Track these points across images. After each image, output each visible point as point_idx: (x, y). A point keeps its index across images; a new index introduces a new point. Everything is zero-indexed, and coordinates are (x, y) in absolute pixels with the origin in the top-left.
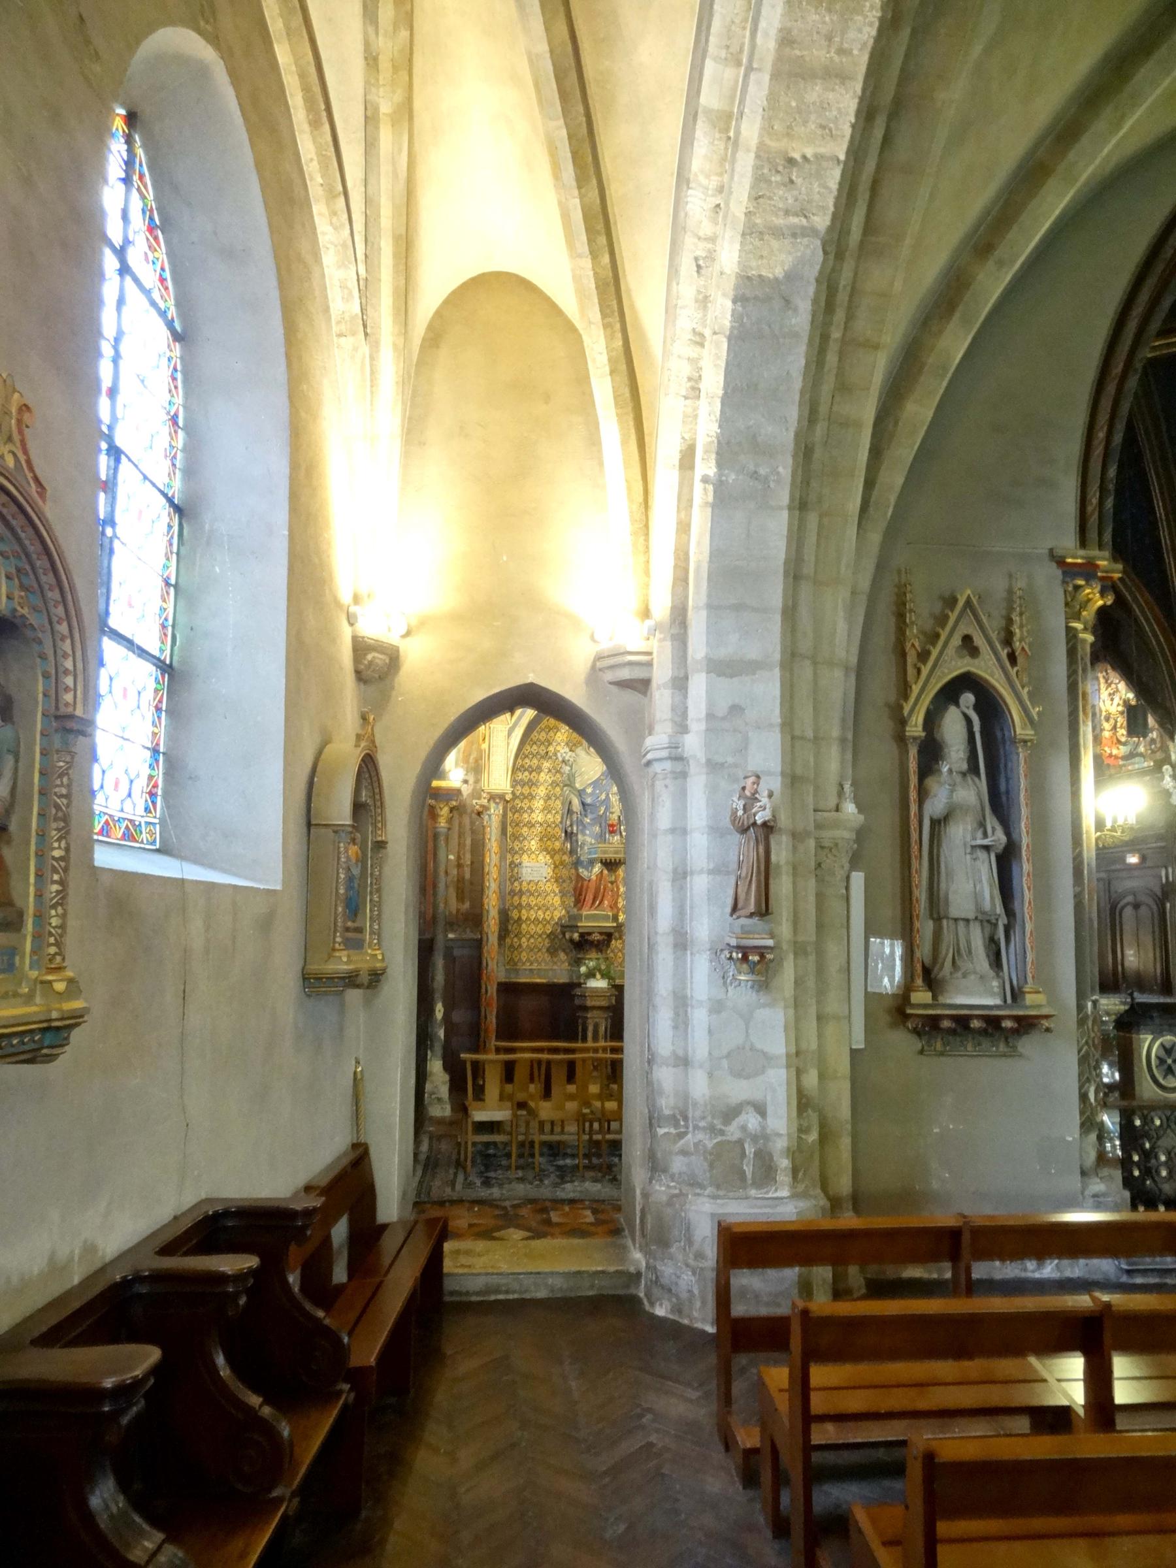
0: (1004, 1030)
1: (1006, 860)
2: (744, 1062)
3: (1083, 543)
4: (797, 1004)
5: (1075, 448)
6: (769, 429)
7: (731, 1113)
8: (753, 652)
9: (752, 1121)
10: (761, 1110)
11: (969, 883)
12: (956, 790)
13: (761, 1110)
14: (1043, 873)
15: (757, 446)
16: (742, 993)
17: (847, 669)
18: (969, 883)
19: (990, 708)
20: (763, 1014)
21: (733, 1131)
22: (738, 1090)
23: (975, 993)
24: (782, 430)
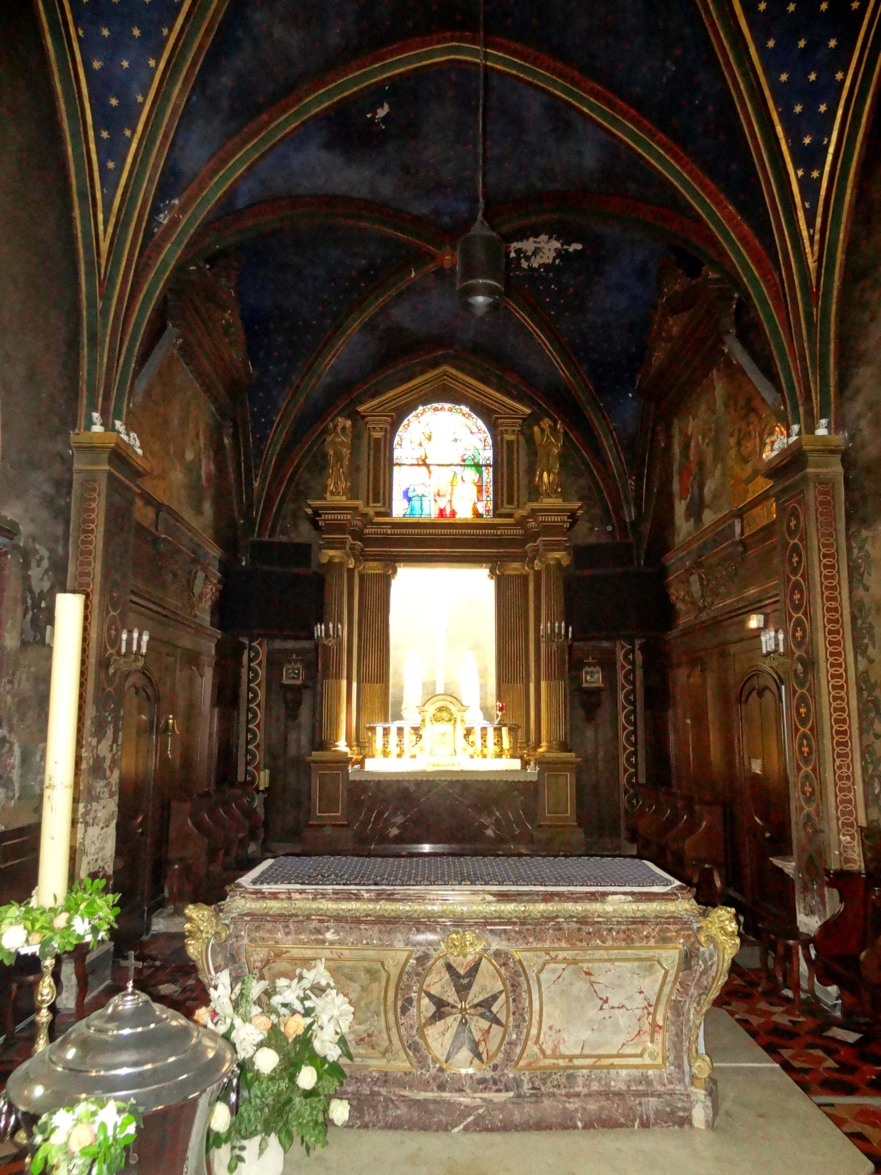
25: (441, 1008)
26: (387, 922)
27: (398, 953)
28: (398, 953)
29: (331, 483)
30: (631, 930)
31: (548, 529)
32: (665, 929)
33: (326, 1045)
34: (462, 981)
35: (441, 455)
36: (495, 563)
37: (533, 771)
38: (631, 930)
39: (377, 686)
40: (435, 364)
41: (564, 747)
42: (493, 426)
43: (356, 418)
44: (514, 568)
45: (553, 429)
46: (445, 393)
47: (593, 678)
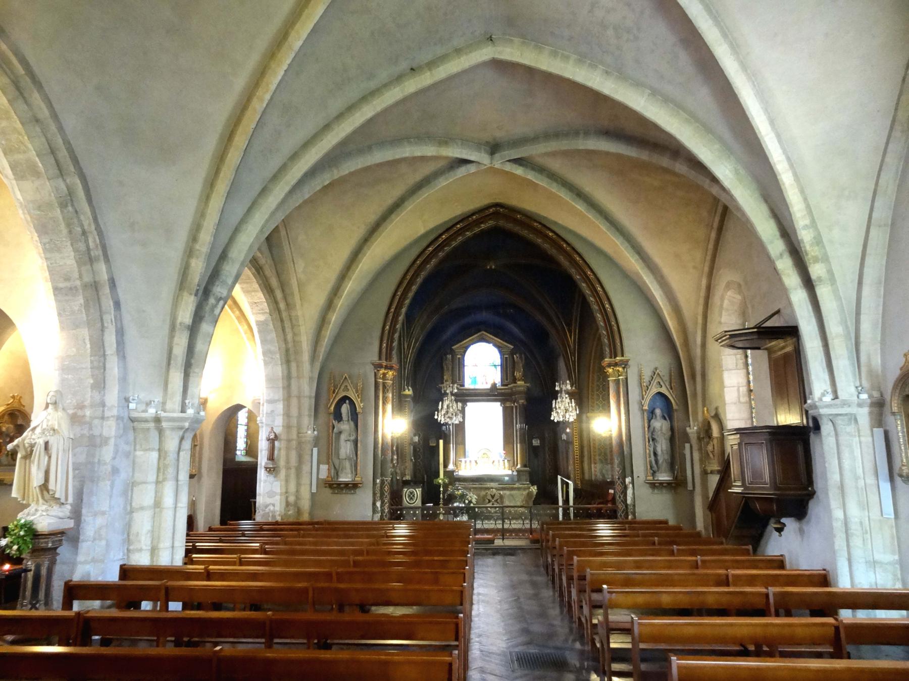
0: (353, 487)
1: (356, 442)
2: (271, 494)
3: (380, 359)
4: (287, 481)
5: (377, 334)
6: (273, 348)
7: (267, 506)
8: (276, 398)
9: (272, 508)
10: (274, 505)
11: (346, 449)
12: (346, 426)
13: (274, 505)
14: (365, 447)
15: (270, 352)
16: (271, 478)
17: (310, 397)
18: (346, 449)
19: (352, 403)
20: (276, 483)
21: (267, 510)
22: (269, 501)
23: (345, 478)
24: (275, 347)
25: (489, 501)
26: (481, 488)
27: (483, 493)
28: (483, 493)
29: (445, 377)
30: (519, 489)
31: (520, 393)
32: (525, 489)
33: (474, 501)
34: (493, 497)
35: (482, 362)
36: (503, 402)
37: (515, 473)
38: (519, 489)
39: (461, 446)
40: (480, 331)
41: (525, 466)
42: (500, 352)
43: (453, 352)
44: (508, 404)
45: (521, 358)
46: (482, 339)
47: (536, 442)
